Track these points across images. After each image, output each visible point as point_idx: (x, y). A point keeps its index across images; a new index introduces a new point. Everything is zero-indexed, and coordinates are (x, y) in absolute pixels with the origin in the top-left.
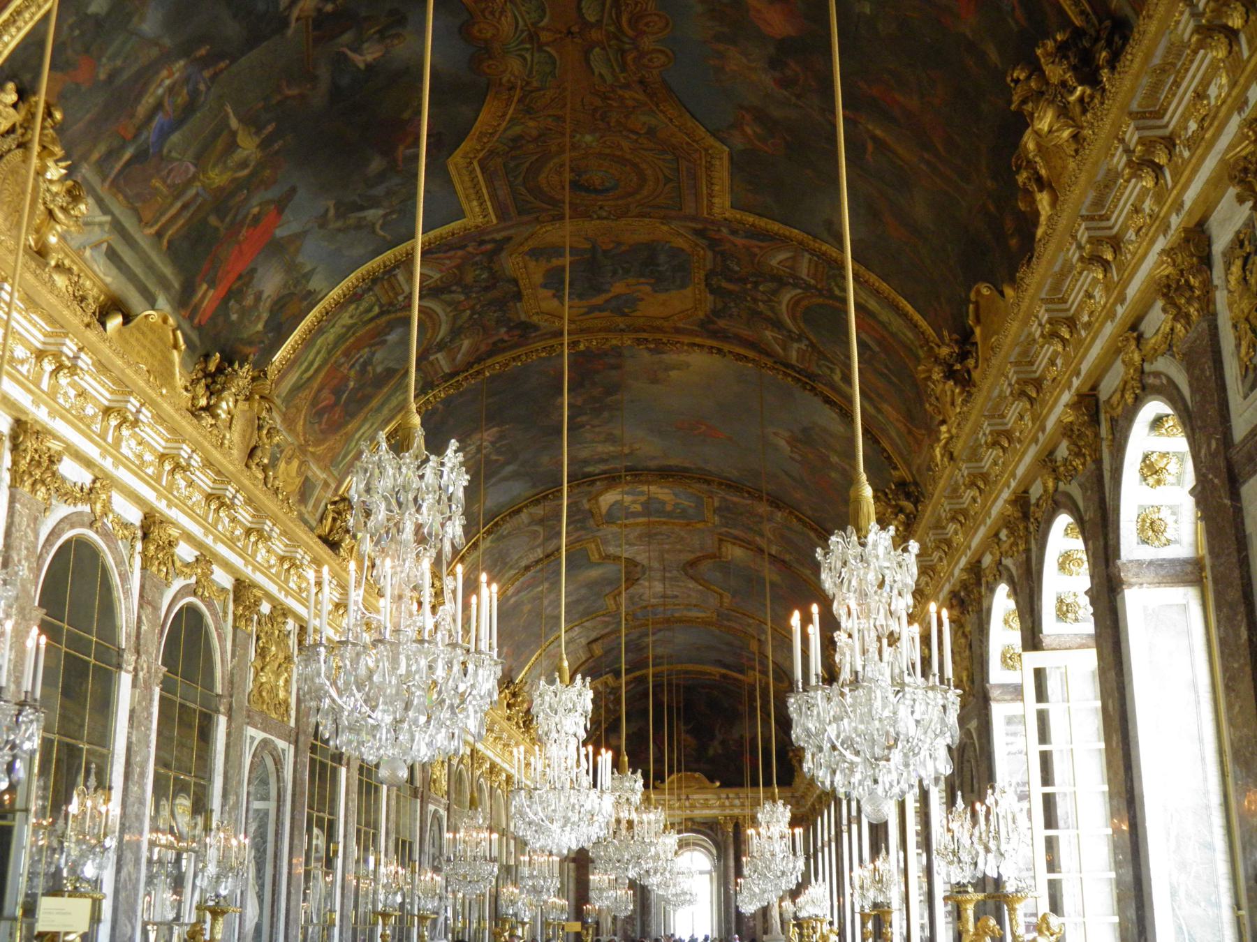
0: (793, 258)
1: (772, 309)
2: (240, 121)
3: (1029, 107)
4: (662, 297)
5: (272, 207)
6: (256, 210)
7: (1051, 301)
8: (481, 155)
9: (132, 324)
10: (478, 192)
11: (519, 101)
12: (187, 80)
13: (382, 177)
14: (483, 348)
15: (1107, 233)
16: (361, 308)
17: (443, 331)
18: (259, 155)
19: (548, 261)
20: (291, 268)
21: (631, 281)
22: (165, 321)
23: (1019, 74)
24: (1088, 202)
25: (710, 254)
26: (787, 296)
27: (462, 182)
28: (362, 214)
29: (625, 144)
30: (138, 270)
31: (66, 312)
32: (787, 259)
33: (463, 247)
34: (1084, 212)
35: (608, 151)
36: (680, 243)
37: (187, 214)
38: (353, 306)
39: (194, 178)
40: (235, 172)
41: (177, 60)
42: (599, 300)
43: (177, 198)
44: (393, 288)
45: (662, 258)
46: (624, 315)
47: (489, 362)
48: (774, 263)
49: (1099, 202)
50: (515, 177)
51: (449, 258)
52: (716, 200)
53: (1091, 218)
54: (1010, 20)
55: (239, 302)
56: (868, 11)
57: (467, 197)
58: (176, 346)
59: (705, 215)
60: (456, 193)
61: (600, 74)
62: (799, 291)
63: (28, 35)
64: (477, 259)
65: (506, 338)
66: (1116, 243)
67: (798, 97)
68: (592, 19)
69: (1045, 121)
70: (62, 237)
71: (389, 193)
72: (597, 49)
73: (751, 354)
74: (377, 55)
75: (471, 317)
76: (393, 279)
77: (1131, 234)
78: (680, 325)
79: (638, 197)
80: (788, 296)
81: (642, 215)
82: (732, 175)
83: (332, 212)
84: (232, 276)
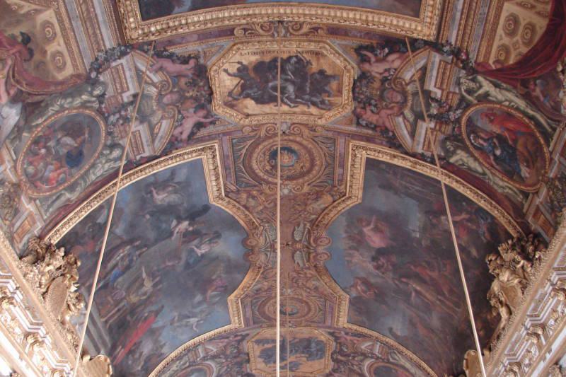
0: (373, 345)
1: (360, 368)
2: (148, 275)
3: (497, 271)
4: (310, 363)
5: (153, 314)
6: (146, 315)
7: (509, 355)
8: (242, 296)
9: (92, 361)
10: (239, 315)
11: (263, 273)
12: (129, 255)
13: (200, 303)
15: (539, 322)
18: (151, 290)
19: (263, 345)
20: (156, 341)
21: (298, 355)
22: (106, 360)
23: (492, 257)
24: (531, 308)
25: (334, 344)
26: (367, 363)
27: (233, 308)
28: (188, 320)
29: (304, 294)
30: (96, 337)
31: (69, 351)
32: (369, 346)
33: (228, 338)
34: (528, 313)
35: (296, 297)
36: (322, 338)
37: (119, 314)
38: (178, 362)
39: (124, 298)
40: (140, 296)
41: (128, 245)
43: (116, 306)
44: (196, 354)
45: (313, 345)
46: (293, 371)
48: (363, 347)
49: (535, 309)
50: (255, 307)
51: (222, 342)
52: (340, 319)
53: (531, 316)
54: (483, 238)
55: (133, 356)
56: (418, 236)
57: (234, 314)
58: (108, 372)
60: (228, 313)
61: (298, 264)
62: (373, 360)
63: (72, 229)
64: (233, 343)
66: (543, 327)
67: (383, 273)
68: (297, 239)
69: (505, 276)
70: (71, 317)
71: (202, 311)
72: (298, 252)
74: (207, 250)
75: (226, 370)
77: (552, 322)
79: (306, 317)
80: (369, 362)
82: (349, 307)
83: (176, 318)
84: (133, 342)
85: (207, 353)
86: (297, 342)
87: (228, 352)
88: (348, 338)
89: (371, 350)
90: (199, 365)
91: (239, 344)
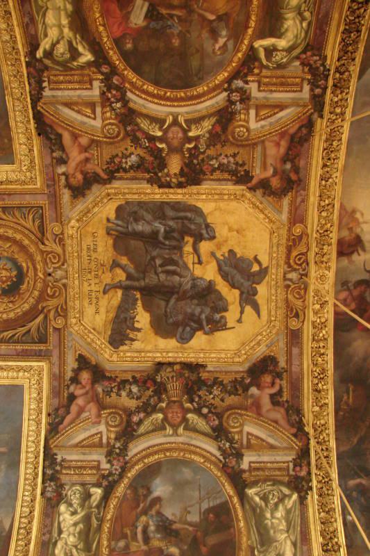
0: (68, 105)
4: (222, 232)
14: (279, 414)
16: (76, 501)
17: (210, 447)
21: (190, 259)
32: (78, 112)
33: (72, 398)
38: (63, 508)
42: (231, 296)
44: (81, 467)
46: (264, 272)
47: (308, 418)
48: (98, 123)
51: (81, 410)
59: (39, 185)
62: (129, 95)
64: (100, 390)
65: (273, 391)
73: (318, 143)
75: (205, 416)
76: (65, 464)
78: (284, 217)
79: (26, 242)
81: (60, 240)
85: (100, 445)
86: (130, 259)
87: (132, 404)
88: (75, 156)
89: (92, 106)
90: (124, 470)
91: (110, 379)
